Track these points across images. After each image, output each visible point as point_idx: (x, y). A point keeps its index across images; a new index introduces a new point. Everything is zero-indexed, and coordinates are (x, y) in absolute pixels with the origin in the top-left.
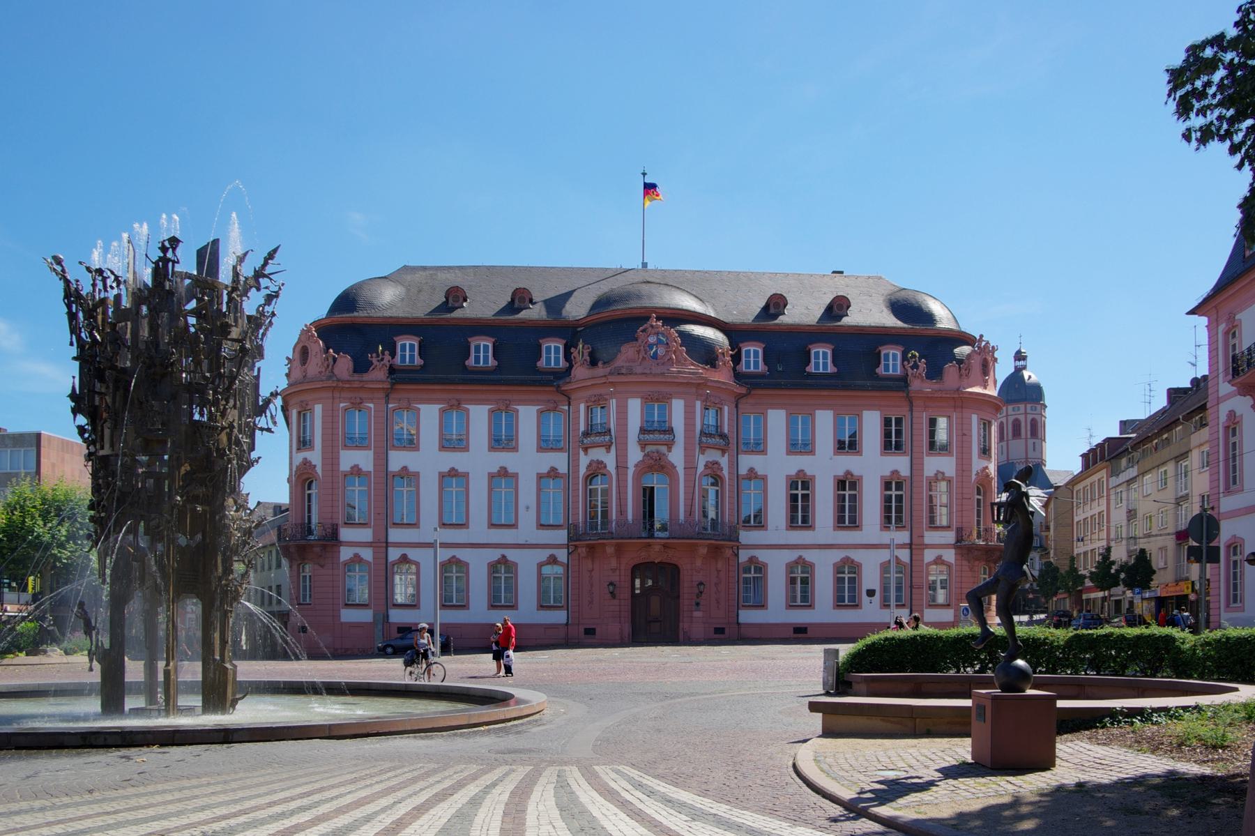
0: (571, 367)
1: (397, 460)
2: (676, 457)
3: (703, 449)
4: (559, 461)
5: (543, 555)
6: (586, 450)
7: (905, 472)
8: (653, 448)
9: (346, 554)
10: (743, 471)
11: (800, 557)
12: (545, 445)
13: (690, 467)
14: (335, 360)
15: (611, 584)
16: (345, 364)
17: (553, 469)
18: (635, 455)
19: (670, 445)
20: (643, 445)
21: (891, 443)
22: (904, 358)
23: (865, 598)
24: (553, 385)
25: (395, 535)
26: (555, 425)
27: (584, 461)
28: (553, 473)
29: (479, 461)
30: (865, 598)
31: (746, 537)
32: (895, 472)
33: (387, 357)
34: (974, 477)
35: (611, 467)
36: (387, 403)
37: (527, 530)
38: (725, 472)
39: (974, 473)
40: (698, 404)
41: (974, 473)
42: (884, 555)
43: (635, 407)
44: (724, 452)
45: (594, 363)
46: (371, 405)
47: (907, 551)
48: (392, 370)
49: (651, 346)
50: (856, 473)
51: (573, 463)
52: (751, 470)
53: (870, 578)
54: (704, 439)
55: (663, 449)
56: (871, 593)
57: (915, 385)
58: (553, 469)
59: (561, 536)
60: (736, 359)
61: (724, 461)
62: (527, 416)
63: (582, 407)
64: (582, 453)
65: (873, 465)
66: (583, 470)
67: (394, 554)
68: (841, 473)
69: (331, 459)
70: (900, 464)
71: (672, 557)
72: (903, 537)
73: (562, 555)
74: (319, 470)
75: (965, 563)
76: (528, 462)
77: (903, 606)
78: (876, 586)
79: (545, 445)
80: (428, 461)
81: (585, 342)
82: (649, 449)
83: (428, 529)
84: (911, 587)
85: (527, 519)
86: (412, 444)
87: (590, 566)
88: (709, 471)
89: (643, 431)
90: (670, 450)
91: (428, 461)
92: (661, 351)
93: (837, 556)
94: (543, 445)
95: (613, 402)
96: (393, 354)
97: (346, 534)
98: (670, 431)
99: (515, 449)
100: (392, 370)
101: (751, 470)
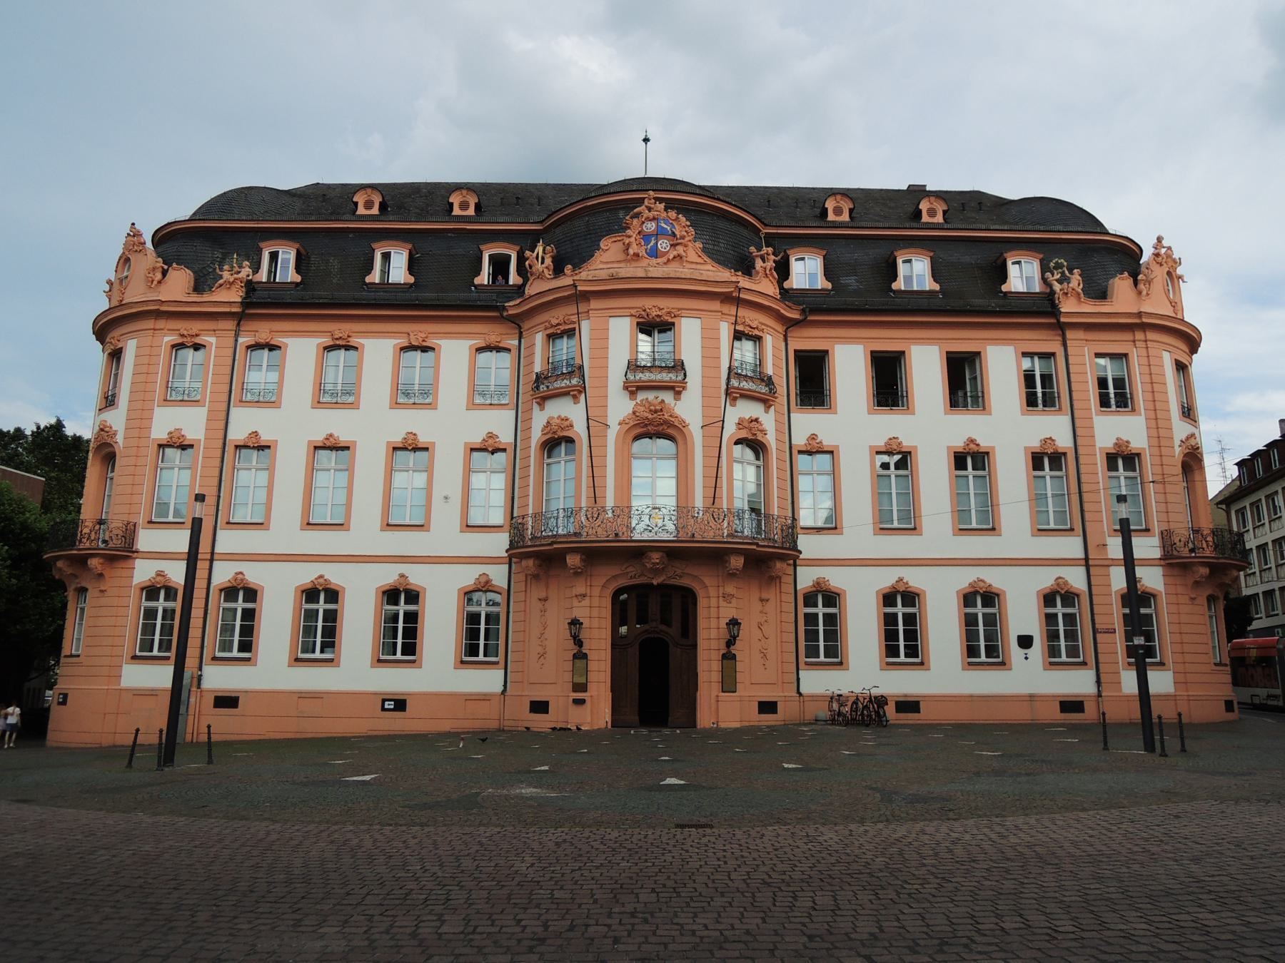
0: (526, 280)
1: (243, 423)
2: (688, 408)
3: (732, 395)
4: (501, 424)
5: (468, 576)
6: (543, 400)
7: (1064, 442)
8: (650, 396)
9: (143, 572)
10: (799, 440)
11: (901, 580)
12: (478, 398)
13: (714, 424)
14: (164, 273)
15: (575, 623)
16: (179, 284)
17: (491, 436)
18: (620, 408)
19: (677, 390)
20: (633, 389)
21: (1039, 393)
22: (1044, 268)
23: (1015, 652)
24: (496, 309)
25: (227, 541)
26: (498, 368)
27: (539, 419)
28: (490, 447)
29: (372, 425)
30: (1015, 652)
31: (808, 546)
32: (1047, 441)
33: (246, 271)
34: (1178, 450)
35: (580, 428)
36: (237, 336)
37: (445, 535)
38: (771, 439)
39: (1177, 443)
40: (725, 330)
41: (1177, 443)
42: (1046, 579)
43: (620, 330)
44: (766, 402)
45: (558, 270)
46: (213, 340)
47: (1082, 570)
48: (250, 286)
49: (646, 237)
50: (984, 443)
51: (522, 425)
52: (813, 437)
53: (1023, 615)
54: (734, 383)
55: (668, 397)
56: (1025, 642)
57: (1068, 306)
58: (491, 436)
59: (499, 544)
60: (783, 270)
61: (768, 421)
62: (455, 351)
63: (539, 338)
64: (535, 406)
65: (1009, 427)
66: (537, 435)
67: (223, 574)
68: (959, 443)
69: (140, 420)
70: (1053, 428)
71: (685, 576)
72: (1071, 546)
73: (499, 574)
74: (120, 438)
75: (1180, 590)
76: (453, 423)
77: (1084, 664)
78: (1034, 627)
79: (478, 398)
80: (291, 423)
81: (546, 244)
82: (641, 396)
83: (285, 533)
84: (1095, 631)
85: (446, 517)
86: (269, 401)
87: (543, 595)
88: (744, 434)
89: (633, 366)
90: (678, 394)
91: (291, 423)
92: (663, 245)
93: (964, 578)
94: (478, 400)
95: (585, 326)
96: (256, 268)
97: (146, 540)
98: (679, 366)
99: (432, 406)
100: (250, 286)
101: (813, 437)
